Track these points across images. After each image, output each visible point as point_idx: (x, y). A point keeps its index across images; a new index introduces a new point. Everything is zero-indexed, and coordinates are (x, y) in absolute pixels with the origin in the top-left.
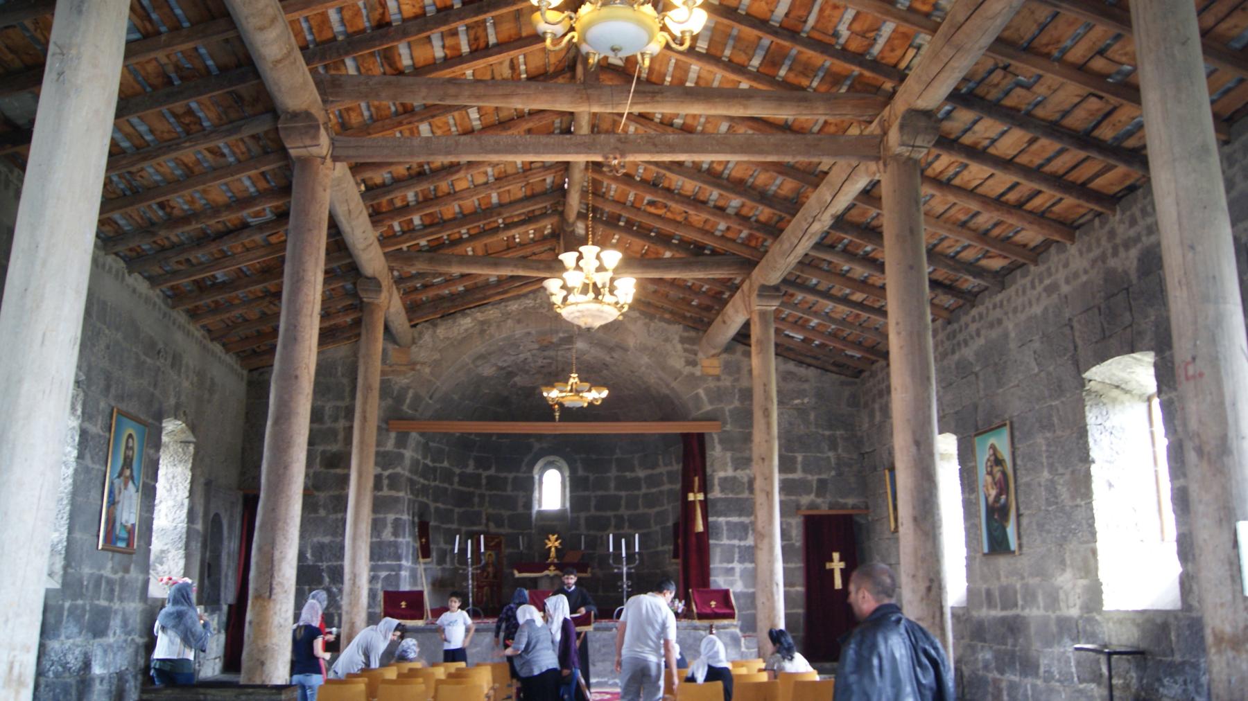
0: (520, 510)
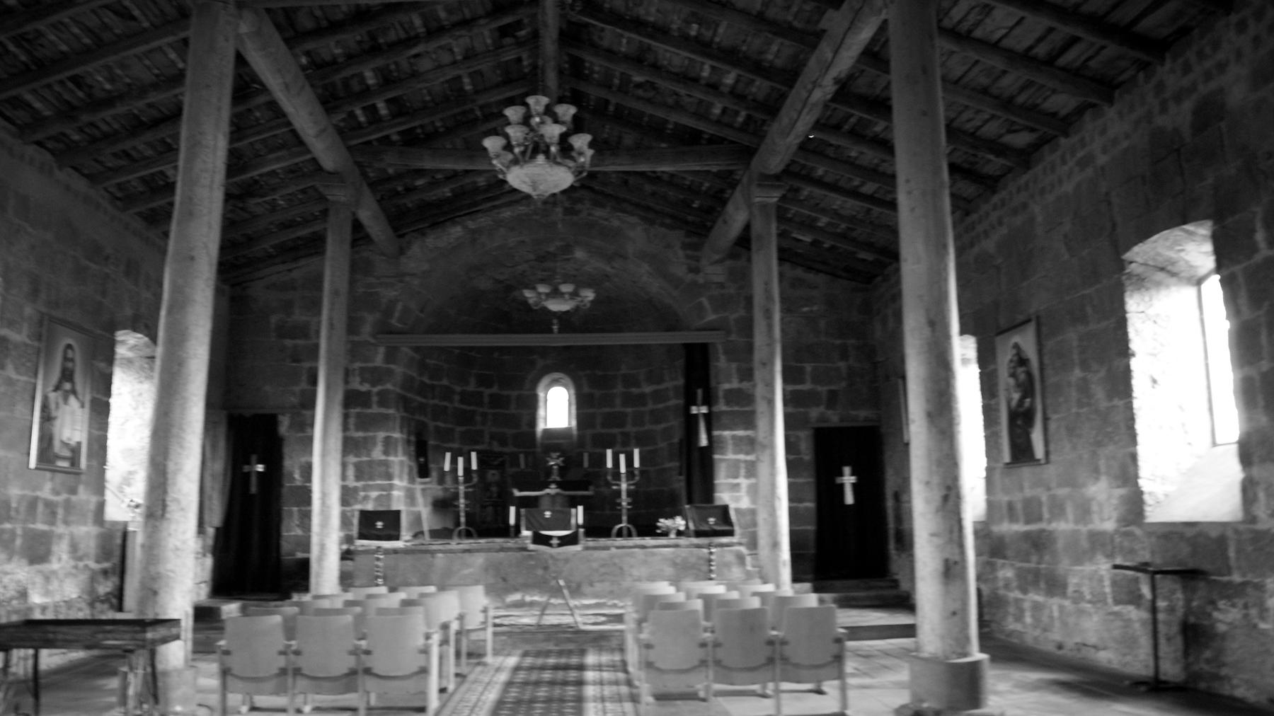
0: (525, 428)
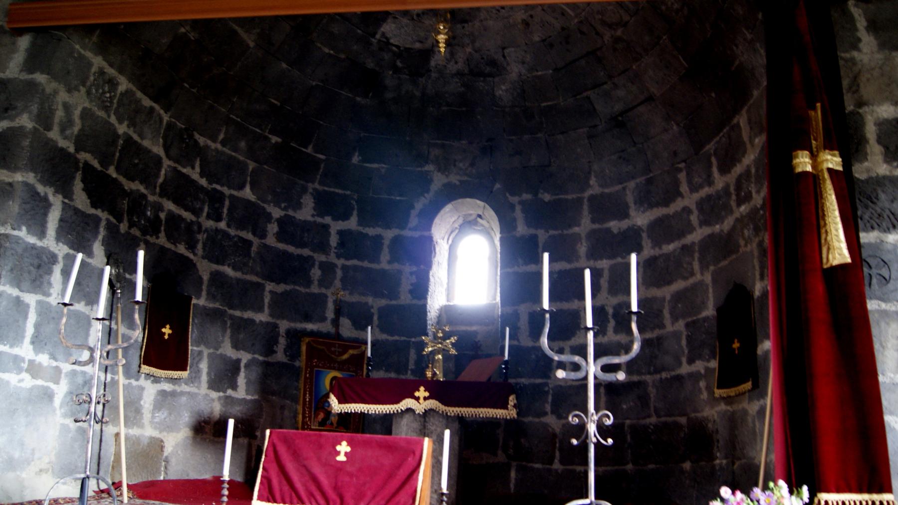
0: (405, 298)
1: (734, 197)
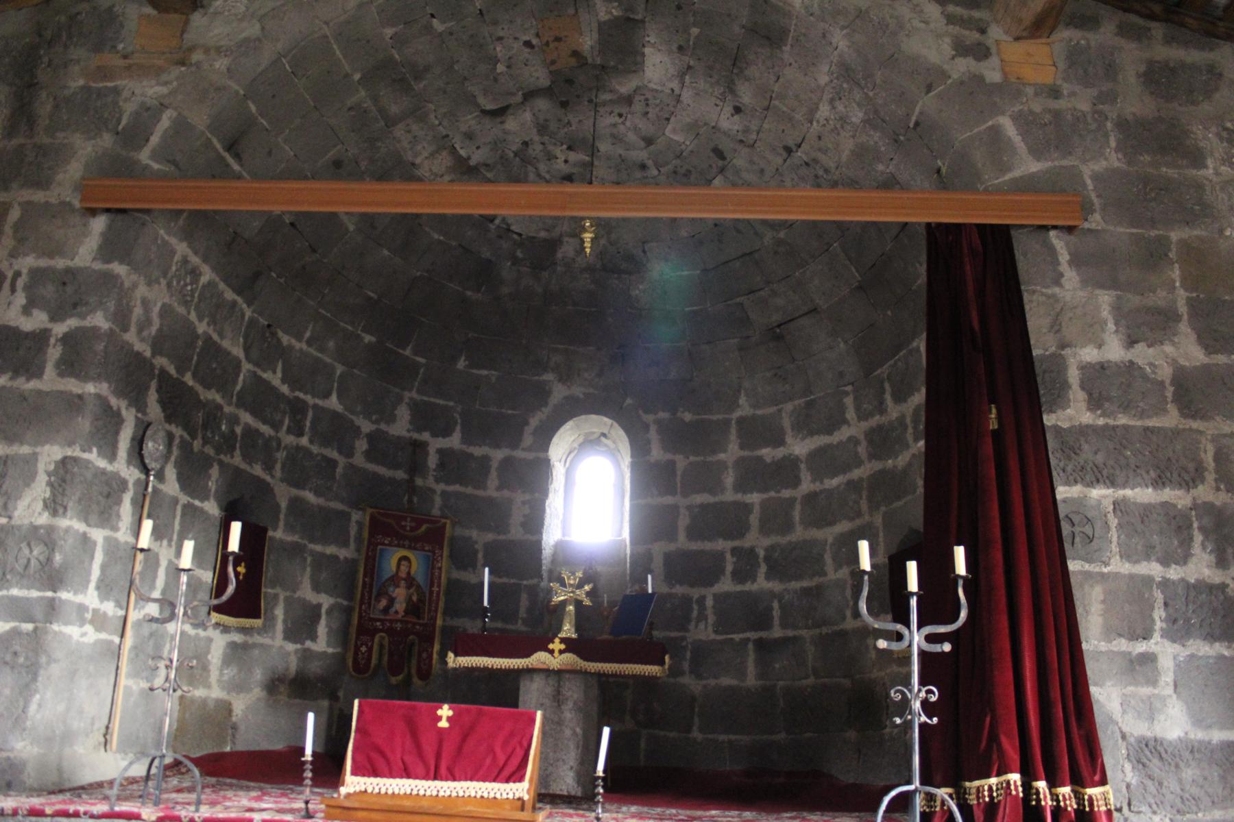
0: (516, 533)
1: (910, 430)
